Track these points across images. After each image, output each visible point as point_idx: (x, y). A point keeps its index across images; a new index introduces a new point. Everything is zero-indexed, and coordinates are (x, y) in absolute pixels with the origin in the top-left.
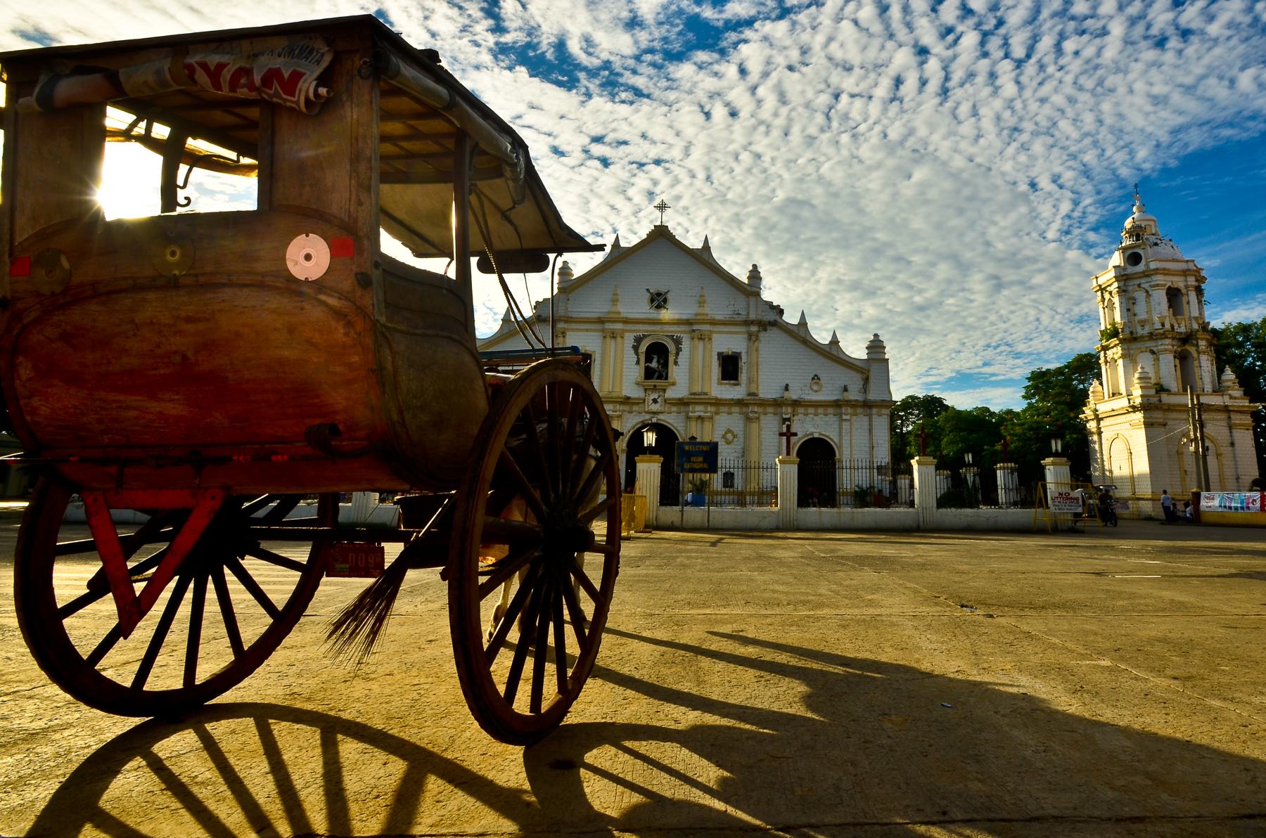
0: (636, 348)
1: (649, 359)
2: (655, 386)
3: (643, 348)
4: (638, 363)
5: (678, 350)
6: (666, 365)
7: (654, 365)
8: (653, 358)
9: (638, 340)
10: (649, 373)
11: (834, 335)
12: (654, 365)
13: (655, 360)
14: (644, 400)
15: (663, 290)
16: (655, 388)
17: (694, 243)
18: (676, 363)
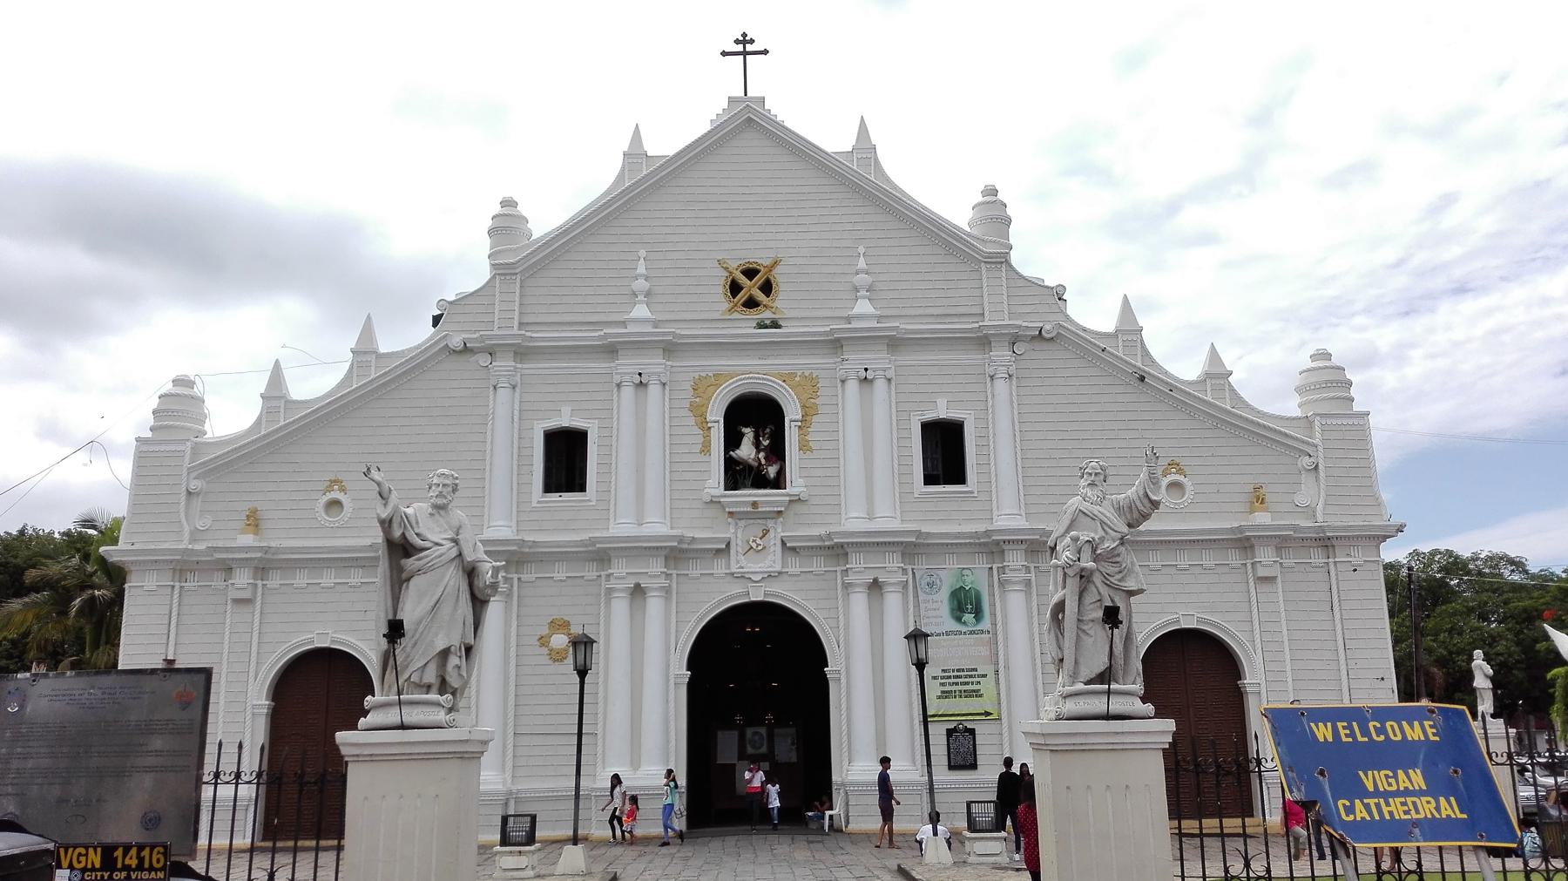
0: (699, 412)
1: (732, 440)
2: (755, 504)
3: (716, 415)
4: (706, 448)
5: (808, 412)
6: (777, 452)
7: (746, 451)
8: (743, 435)
9: (702, 388)
10: (737, 475)
11: (1214, 355)
12: (746, 451)
13: (749, 433)
14: (728, 545)
15: (761, 258)
16: (754, 514)
17: (834, 139)
18: (804, 447)
